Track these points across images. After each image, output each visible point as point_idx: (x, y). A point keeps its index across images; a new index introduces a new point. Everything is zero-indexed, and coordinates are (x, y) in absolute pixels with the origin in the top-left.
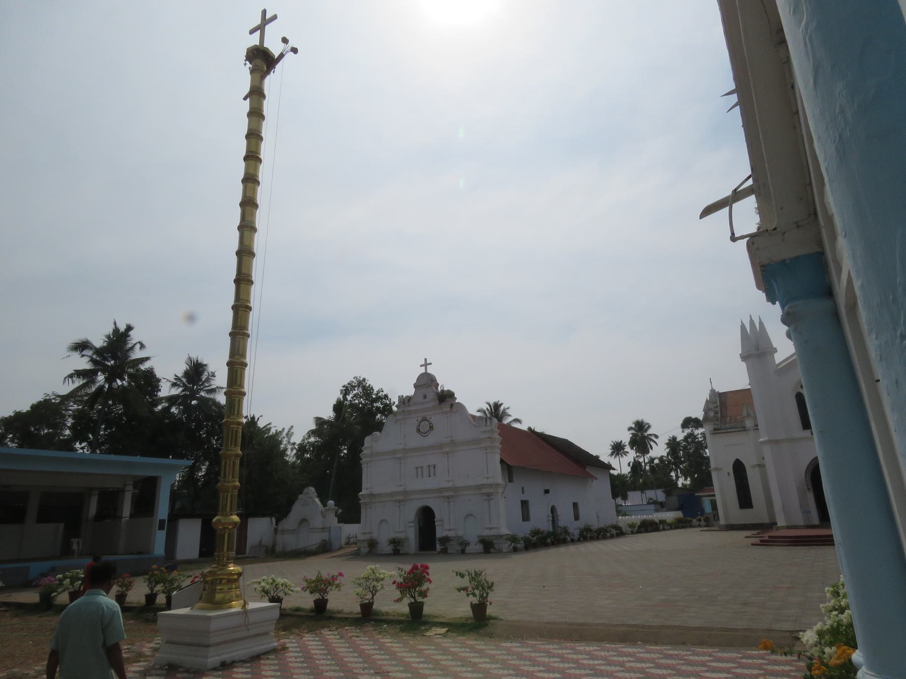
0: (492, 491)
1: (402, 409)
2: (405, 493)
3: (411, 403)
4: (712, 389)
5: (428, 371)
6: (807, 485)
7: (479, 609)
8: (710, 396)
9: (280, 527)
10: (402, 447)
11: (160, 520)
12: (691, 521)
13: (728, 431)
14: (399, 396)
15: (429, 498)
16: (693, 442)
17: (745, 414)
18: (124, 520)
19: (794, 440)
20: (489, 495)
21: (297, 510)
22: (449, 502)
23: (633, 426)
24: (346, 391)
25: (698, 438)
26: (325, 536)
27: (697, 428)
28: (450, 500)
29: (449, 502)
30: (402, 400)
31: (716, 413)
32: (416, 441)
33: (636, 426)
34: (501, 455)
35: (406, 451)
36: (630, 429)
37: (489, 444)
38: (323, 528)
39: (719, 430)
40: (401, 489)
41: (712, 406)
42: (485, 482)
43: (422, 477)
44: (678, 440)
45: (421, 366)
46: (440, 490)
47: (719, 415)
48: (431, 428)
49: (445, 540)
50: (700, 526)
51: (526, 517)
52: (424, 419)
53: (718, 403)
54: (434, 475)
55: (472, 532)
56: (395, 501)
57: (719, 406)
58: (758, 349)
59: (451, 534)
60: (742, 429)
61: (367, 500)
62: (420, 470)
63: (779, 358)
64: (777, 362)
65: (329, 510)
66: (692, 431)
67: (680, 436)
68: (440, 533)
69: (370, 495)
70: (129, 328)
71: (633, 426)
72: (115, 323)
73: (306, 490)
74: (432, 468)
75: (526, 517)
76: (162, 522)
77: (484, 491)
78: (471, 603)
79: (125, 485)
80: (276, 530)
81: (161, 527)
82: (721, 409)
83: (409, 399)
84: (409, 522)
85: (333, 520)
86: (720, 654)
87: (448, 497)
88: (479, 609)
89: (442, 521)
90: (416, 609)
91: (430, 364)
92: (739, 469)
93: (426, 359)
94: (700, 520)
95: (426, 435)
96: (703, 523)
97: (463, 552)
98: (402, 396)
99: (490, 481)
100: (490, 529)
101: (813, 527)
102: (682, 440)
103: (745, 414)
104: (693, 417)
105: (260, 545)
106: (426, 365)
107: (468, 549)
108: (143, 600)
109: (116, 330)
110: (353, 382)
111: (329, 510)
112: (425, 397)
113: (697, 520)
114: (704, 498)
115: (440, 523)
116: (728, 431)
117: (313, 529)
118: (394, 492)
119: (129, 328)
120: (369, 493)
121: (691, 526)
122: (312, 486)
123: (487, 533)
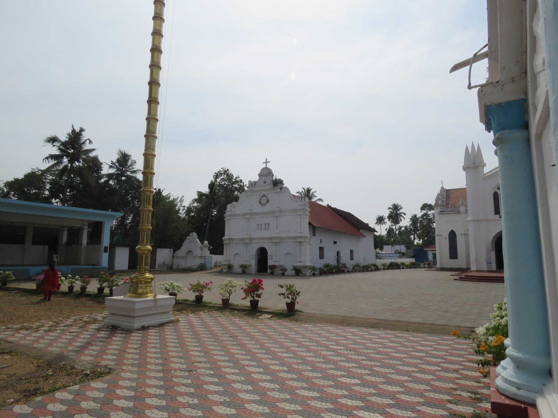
0: (301, 240)
1: (250, 189)
2: (250, 239)
3: (256, 186)
4: (442, 187)
6: (492, 248)
7: (291, 306)
8: (441, 191)
9: (175, 254)
10: (249, 212)
11: (104, 247)
12: (420, 264)
13: (450, 213)
14: (249, 181)
15: (265, 242)
16: (426, 218)
17: (460, 203)
18: (83, 245)
19: (488, 220)
20: (300, 242)
21: (186, 246)
22: (276, 245)
23: (392, 207)
24: (217, 176)
25: (430, 216)
26: (202, 261)
27: (430, 210)
28: (277, 244)
29: (276, 245)
30: (251, 184)
31: (443, 202)
32: (258, 208)
33: (393, 207)
34: (309, 219)
35: (251, 214)
36: (389, 208)
37: (303, 213)
38: (201, 257)
39: (443, 212)
40: (248, 236)
41: (441, 197)
42: (299, 235)
43: (261, 230)
44: (417, 217)
45: (264, 163)
46: (271, 238)
47: (445, 203)
48: (268, 201)
49: (273, 267)
50: (424, 267)
51: (322, 257)
52: (264, 196)
53: (445, 196)
54: (268, 229)
55: (289, 264)
56: (245, 243)
57: (445, 198)
58: (474, 163)
59: (276, 264)
60: (458, 212)
61: (227, 242)
62: (260, 226)
63: (486, 170)
64: (485, 173)
65: (205, 246)
66: (427, 212)
67: (419, 214)
68: (270, 263)
69: (229, 239)
70: (82, 130)
71: (392, 207)
72: (73, 126)
73: (191, 234)
74: (267, 225)
75: (322, 257)
76: (106, 248)
77: (298, 240)
78: (286, 302)
79: (83, 226)
80: (173, 256)
81: (105, 251)
82: (446, 200)
83: (255, 183)
84: (252, 256)
85: (207, 252)
86: (428, 338)
87: (276, 243)
88: (291, 306)
89: (271, 256)
90: (254, 304)
91: (269, 162)
92: (452, 236)
93: (266, 159)
94: (425, 264)
95: (264, 205)
96: (426, 266)
97: (283, 274)
99: (302, 235)
100: (300, 262)
101: (492, 272)
102: (420, 217)
103: (460, 203)
104: (429, 203)
105: (164, 264)
106: (266, 162)
107: (286, 273)
108: (96, 291)
109: (74, 131)
110: (221, 171)
111: (205, 246)
112: (265, 182)
113: (423, 264)
114: (429, 252)
115: (270, 257)
116: (450, 213)
117: (195, 256)
118: (244, 238)
119: (82, 130)
120: (229, 238)
121: (419, 267)
122: (195, 232)
123: (298, 264)
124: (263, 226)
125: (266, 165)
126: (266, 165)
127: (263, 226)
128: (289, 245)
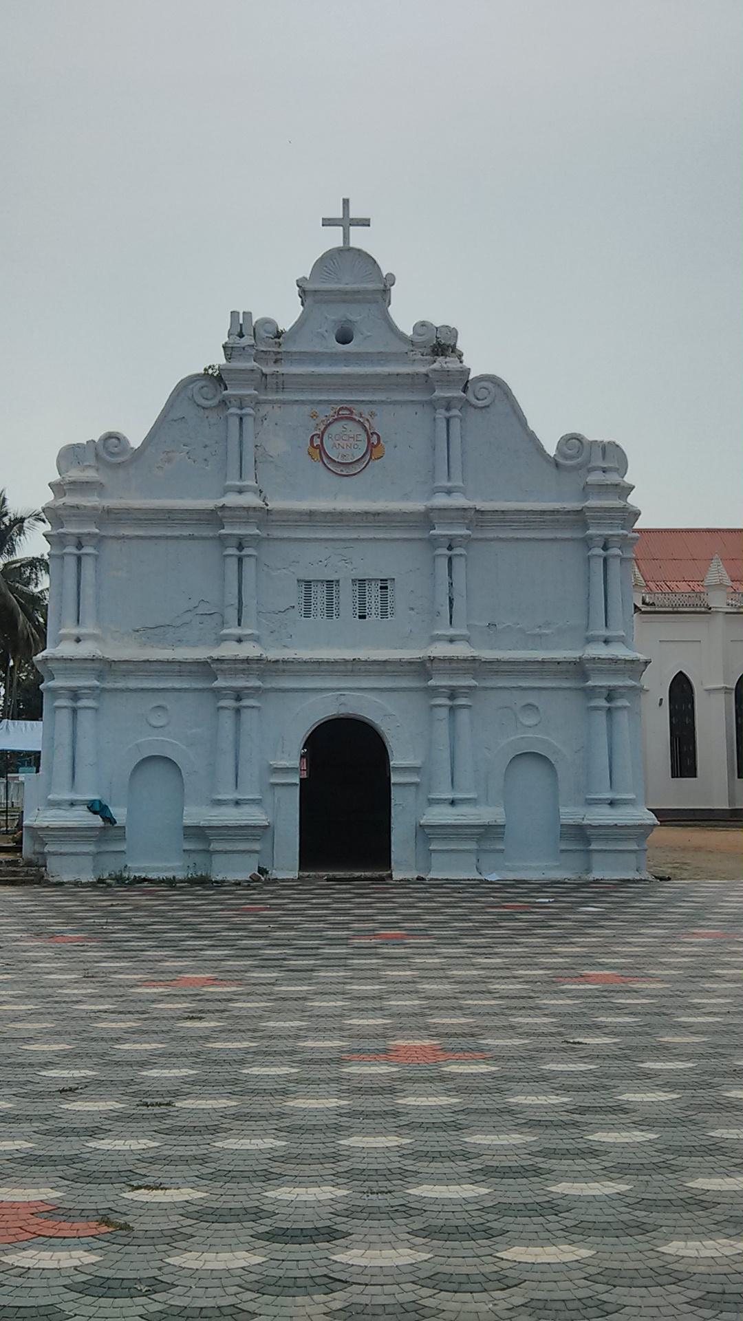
5: (352, 245)
14: (234, 314)
45: (327, 222)
48: (373, 448)
52: (345, 414)
54: (384, 614)
62: (319, 593)
74: (374, 592)
92: (681, 690)
93: (346, 202)
98: (247, 315)
106: (347, 222)
124: (347, 597)
125: (346, 237)
126: (346, 237)
127: (347, 597)
128: (530, 706)
